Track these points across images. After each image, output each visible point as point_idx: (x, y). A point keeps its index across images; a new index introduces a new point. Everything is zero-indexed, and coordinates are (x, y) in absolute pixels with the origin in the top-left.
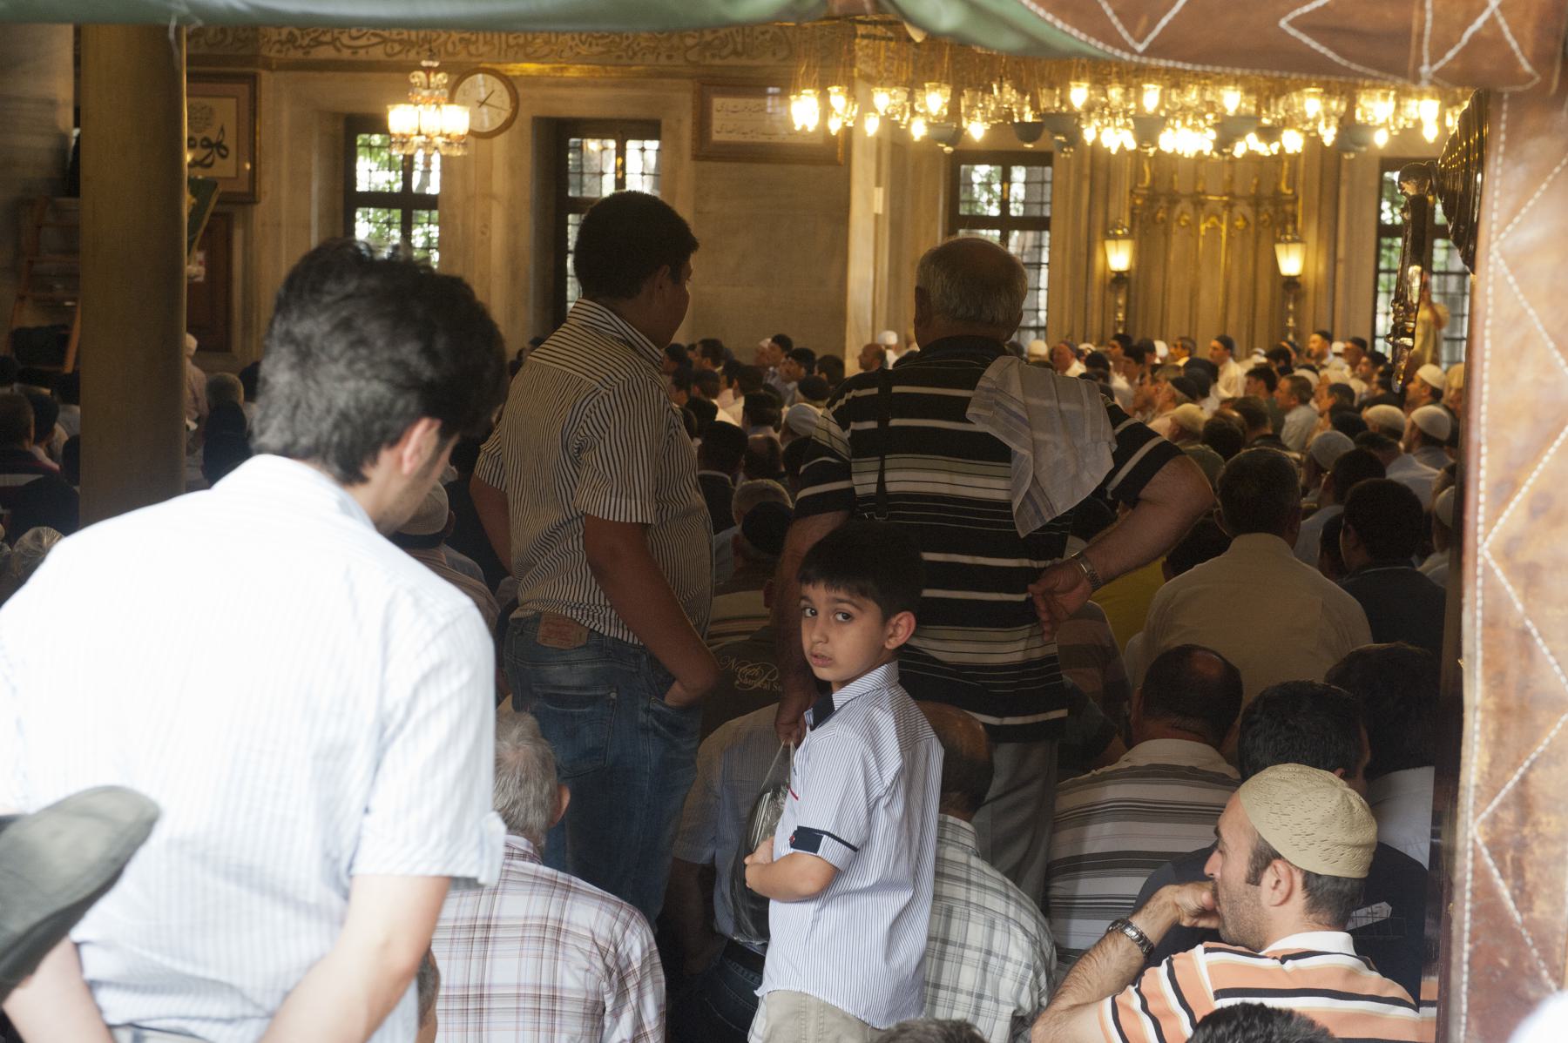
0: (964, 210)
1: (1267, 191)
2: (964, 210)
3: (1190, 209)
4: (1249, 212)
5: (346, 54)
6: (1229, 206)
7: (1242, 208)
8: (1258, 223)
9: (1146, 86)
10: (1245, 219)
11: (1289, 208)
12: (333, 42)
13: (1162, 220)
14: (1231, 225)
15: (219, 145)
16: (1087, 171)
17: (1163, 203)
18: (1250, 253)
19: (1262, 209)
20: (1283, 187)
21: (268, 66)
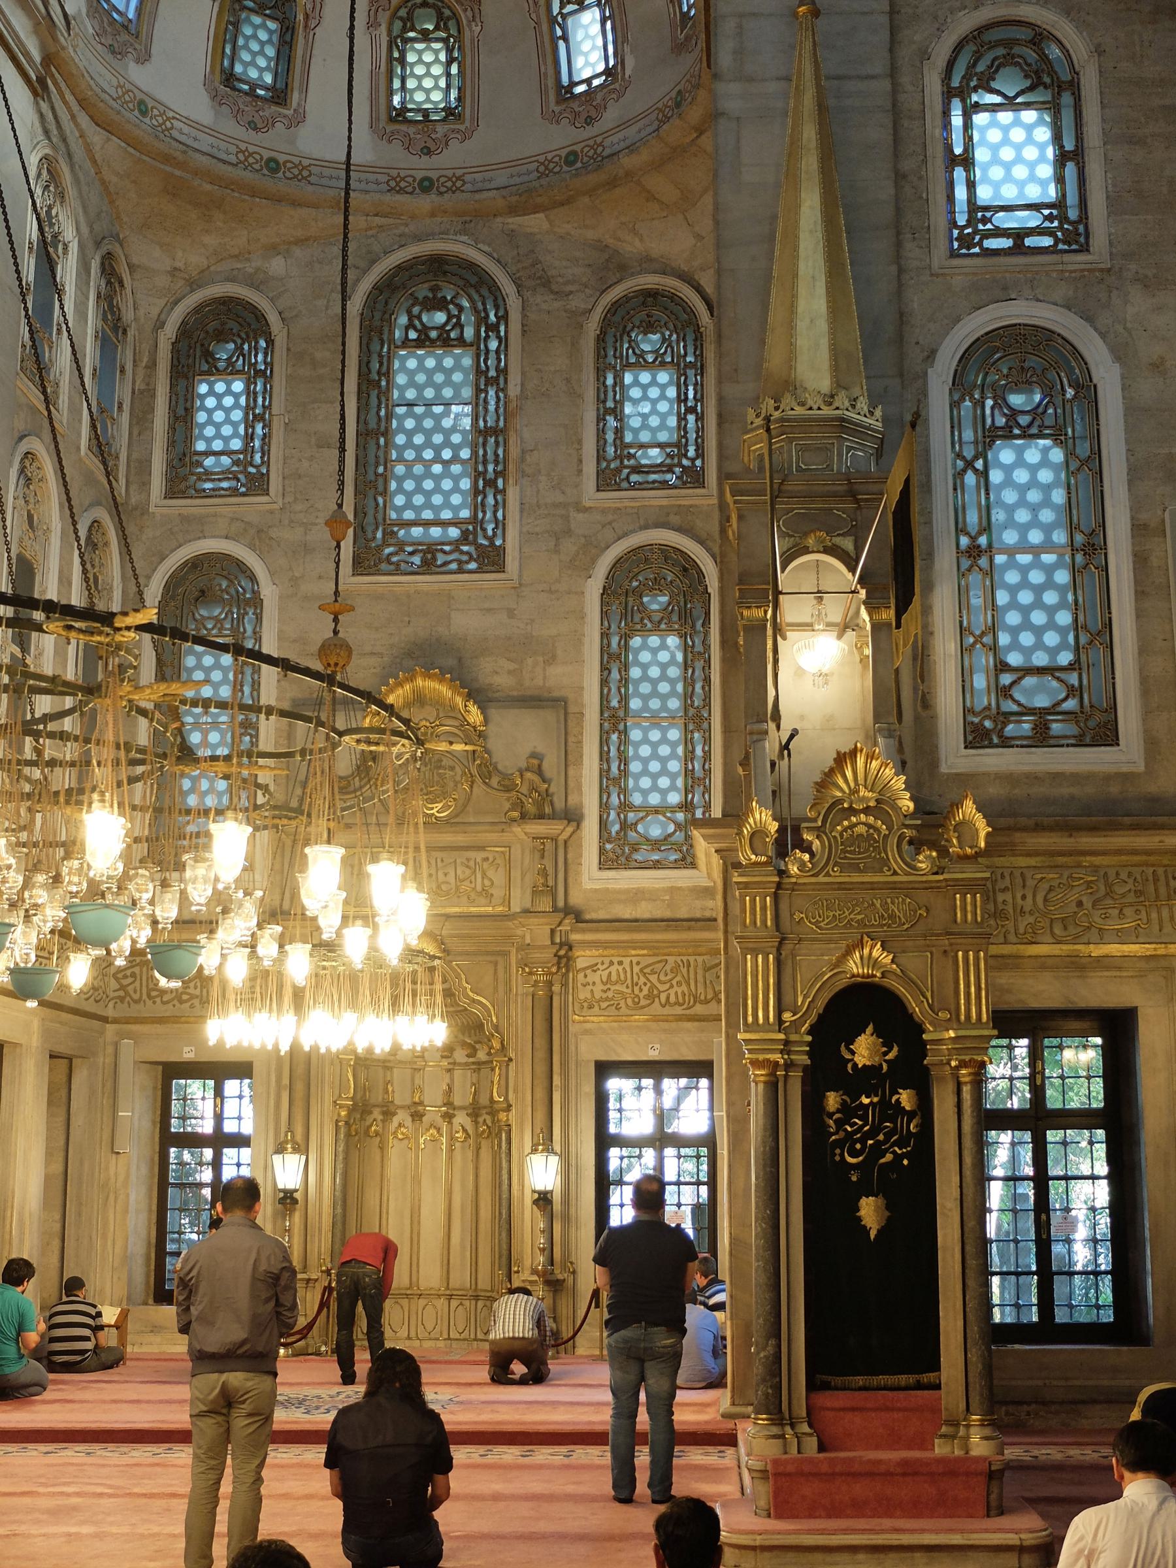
0: (175, 1126)
1: (484, 1100)
2: (175, 1126)
3: (408, 1121)
4: (468, 1123)
6: (448, 1117)
7: (461, 1119)
8: (479, 1135)
10: (465, 1130)
11: (502, 1116)
13: (377, 1134)
14: (452, 1138)
16: (286, 1081)
17: (377, 1114)
18: (471, 1166)
19: (481, 1120)
20: (496, 1098)
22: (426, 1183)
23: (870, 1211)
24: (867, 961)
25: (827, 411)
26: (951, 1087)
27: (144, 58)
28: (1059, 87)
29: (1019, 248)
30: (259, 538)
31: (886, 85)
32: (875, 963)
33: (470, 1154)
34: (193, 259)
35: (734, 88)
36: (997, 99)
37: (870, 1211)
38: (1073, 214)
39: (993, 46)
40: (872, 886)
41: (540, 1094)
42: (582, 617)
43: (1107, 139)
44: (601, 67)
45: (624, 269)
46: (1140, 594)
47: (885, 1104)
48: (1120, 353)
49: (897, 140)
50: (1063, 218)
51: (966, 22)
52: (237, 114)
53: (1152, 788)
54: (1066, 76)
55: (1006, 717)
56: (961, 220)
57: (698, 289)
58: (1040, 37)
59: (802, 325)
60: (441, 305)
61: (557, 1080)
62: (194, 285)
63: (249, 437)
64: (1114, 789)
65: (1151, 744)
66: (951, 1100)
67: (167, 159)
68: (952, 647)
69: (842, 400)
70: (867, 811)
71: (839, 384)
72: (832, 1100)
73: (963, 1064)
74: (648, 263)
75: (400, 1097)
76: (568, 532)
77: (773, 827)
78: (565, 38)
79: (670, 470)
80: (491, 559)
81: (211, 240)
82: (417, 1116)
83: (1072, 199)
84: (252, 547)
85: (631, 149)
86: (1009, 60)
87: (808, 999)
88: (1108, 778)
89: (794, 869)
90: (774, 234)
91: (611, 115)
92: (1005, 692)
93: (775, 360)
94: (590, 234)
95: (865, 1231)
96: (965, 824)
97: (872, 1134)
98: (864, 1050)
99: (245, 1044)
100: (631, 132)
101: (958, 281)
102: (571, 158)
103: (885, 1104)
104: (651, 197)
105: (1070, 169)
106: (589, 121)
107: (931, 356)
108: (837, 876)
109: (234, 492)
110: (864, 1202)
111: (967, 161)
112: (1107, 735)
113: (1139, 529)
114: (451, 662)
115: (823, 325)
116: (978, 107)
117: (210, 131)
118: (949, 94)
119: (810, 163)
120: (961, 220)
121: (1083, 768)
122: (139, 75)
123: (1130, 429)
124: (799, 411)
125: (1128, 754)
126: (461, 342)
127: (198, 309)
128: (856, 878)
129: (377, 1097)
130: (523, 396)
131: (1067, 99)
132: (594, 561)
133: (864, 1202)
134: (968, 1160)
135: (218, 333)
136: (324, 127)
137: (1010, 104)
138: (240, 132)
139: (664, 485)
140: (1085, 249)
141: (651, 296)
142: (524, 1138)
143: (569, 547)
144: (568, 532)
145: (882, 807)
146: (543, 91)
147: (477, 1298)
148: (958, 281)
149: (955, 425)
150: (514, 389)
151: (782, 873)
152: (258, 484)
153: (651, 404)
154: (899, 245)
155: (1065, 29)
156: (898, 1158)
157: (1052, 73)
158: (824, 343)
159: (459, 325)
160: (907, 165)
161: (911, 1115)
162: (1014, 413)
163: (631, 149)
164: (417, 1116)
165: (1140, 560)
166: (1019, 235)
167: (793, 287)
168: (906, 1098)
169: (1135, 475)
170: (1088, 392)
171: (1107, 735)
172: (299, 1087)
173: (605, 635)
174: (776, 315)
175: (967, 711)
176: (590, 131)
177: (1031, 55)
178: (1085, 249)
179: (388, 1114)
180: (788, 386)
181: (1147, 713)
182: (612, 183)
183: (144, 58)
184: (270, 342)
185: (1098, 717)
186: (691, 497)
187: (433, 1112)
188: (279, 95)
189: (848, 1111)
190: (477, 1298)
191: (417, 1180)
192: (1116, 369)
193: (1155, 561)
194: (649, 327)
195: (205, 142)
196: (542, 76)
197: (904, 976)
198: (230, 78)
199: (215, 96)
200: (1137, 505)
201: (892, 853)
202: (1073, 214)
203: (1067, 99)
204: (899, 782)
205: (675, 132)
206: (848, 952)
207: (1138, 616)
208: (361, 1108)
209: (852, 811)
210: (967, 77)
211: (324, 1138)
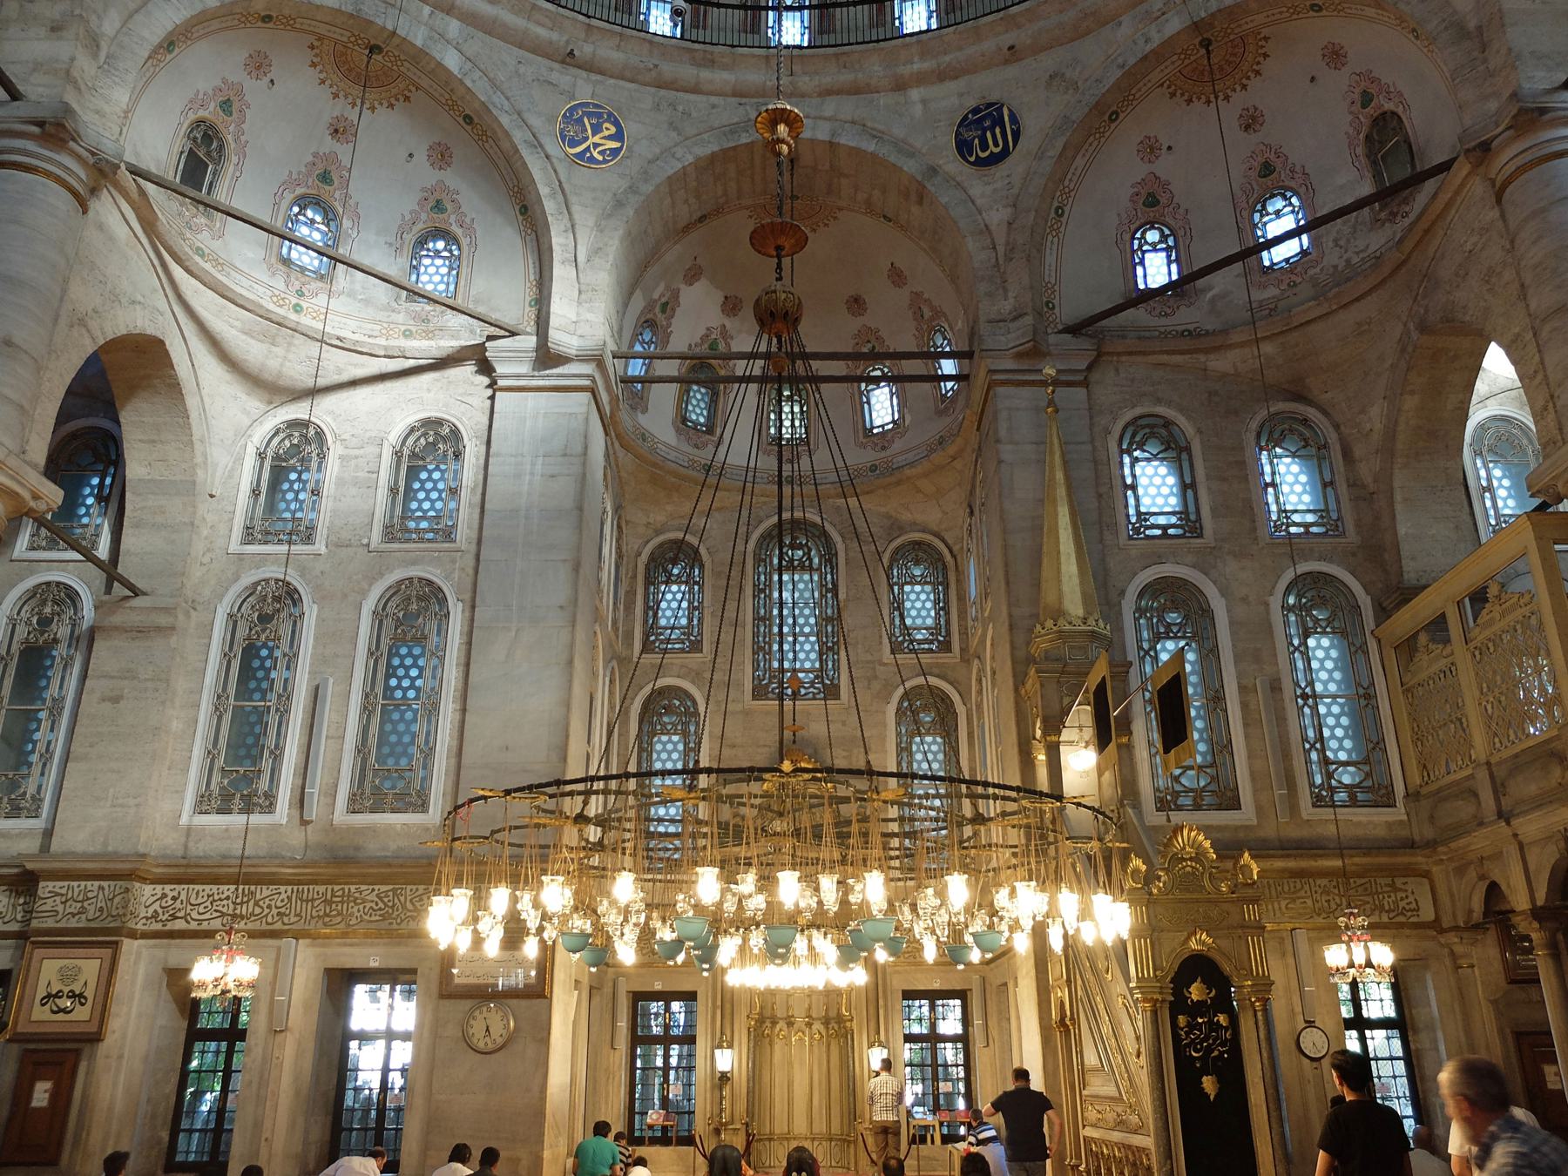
1: (833, 1014)
5: (193, 926)
6: (809, 1025)
7: (817, 1026)
9: (780, 875)
12: (184, 918)
14: (811, 1038)
15: (81, 996)
21: (133, 935)
22: (796, 1066)
23: (1209, 1084)
24: (1199, 942)
25: (1083, 628)
26: (1251, 1013)
27: (645, 410)
28: (1181, 450)
29: (1165, 535)
30: (696, 677)
31: (1089, 447)
32: (1203, 943)
33: (824, 1049)
34: (659, 518)
35: (1009, 447)
36: (1147, 455)
37: (1209, 1084)
38: (1193, 517)
39: (1143, 427)
40: (1197, 901)
41: (872, 1011)
42: (885, 725)
43: (1208, 477)
44: (889, 419)
45: (902, 530)
46: (1246, 725)
47: (1210, 1022)
48: (1224, 592)
49: (1097, 477)
50: (1188, 520)
51: (1129, 415)
52: (689, 439)
53: (1262, 834)
54: (1183, 444)
55: (1176, 794)
56: (1133, 520)
57: (943, 540)
58: (1168, 424)
59: (1065, 579)
60: (800, 547)
61: (881, 1002)
62: (658, 532)
63: (690, 620)
64: (1241, 835)
65: (1259, 810)
66: (1251, 1023)
67: (655, 465)
68: (1145, 754)
69: (1091, 621)
70: (1191, 859)
71: (1088, 613)
72: (1182, 1020)
73: (1258, 1000)
74: (914, 526)
75: (780, 1013)
76: (876, 677)
77: (1144, 868)
78: (868, 403)
79: (931, 642)
80: (831, 692)
81: (669, 508)
82: (790, 1024)
83: (1192, 508)
84: (693, 682)
85: (911, 464)
86: (1153, 435)
87: (1170, 965)
88: (1237, 828)
89: (1155, 891)
90: (1039, 530)
91: (898, 445)
92: (1176, 779)
93: (1049, 597)
94: (883, 510)
95: (1208, 1096)
96: (1247, 866)
97: (1206, 1039)
98: (1196, 992)
99: (773, 987)
100: (910, 456)
101: (1134, 552)
102: (873, 468)
103: (1210, 1022)
104: (919, 491)
105: (1190, 493)
106: (884, 448)
107: (1122, 593)
108: (1178, 895)
109: (682, 651)
110: (1205, 1079)
111: (1134, 487)
112: (1235, 805)
113: (1243, 689)
114: (810, 751)
115: (1076, 580)
116: (1137, 460)
117: (676, 449)
118: (1122, 452)
119: (1061, 492)
120: (1133, 520)
121: (1223, 823)
122: (642, 419)
123: (1233, 634)
124: (1068, 627)
125: (1247, 815)
126: (811, 569)
127: (661, 545)
128: (1188, 896)
129: (768, 1013)
130: (847, 600)
131: (1184, 456)
132: (890, 695)
133: (1205, 1079)
134: (1265, 1055)
135: (674, 557)
136: (739, 448)
137: (1155, 457)
138: (690, 450)
139: (931, 651)
140: (1200, 536)
141: (918, 544)
142: (861, 1039)
143: (876, 686)
144: (876, 677)
145: (1199, 856)
146: (856, 432)
147: (831, 1140)
148: (1134, 552)
149: (1138, 630)
150: (842, 596)
151: (1151, 894)
152: (696, 646)
153: (920, 605)
154: (1101, 532)
155: (1182, 421)
156: (1222, 1053)
157: (1176, 442)
158: (1078, 589)
159: (810, 559)
160: (1103, 490)
161: (1226, 1029)
162: (1169, 626)
163: (911, 464)
164: (790, 1024)
165: (1244, 706)
166: (1165, 528)
167: (1058, 559)
168: (1222, 1019)
169: (1238, 659)
170: (1207, 613)
171: (1235, 805)
172: (728, 1006)
173: (899, 734)
174: (1047, 572)
175: (1157, 790)
176: (883, 454)
177: (1163, 432)
178: (1200, 536)
179: (774, 1023)
180: (1058, 613)
181: (1255, 791)
182: (898, 483)
183: (645, 410)
184: (702, 567)
185: (1229, 794)
186: (944, 658)
187: (800, 1021)
188: (710, 430)
189: (1192, 1026)
190: (831, 1140)
191: (790, 1064)
192: (1223, 601)
193: (1252, 707)
194: (917, 563)
195: (672, 455)
196: (855, 423)
197: (1219, 950)
198: (684, 420)
199: (678, 430)
200: (1240, 676)
201: (1206, 883)
202: (1193, 517)
203: (1184, 456)
204: (1207, 844)
205: (938, 458)
206: (1188, 938)
207: (1246, 737)
208: (761, 1021)
209: (1184, 860)
210: (1131, 444)
211: (742, 1037)
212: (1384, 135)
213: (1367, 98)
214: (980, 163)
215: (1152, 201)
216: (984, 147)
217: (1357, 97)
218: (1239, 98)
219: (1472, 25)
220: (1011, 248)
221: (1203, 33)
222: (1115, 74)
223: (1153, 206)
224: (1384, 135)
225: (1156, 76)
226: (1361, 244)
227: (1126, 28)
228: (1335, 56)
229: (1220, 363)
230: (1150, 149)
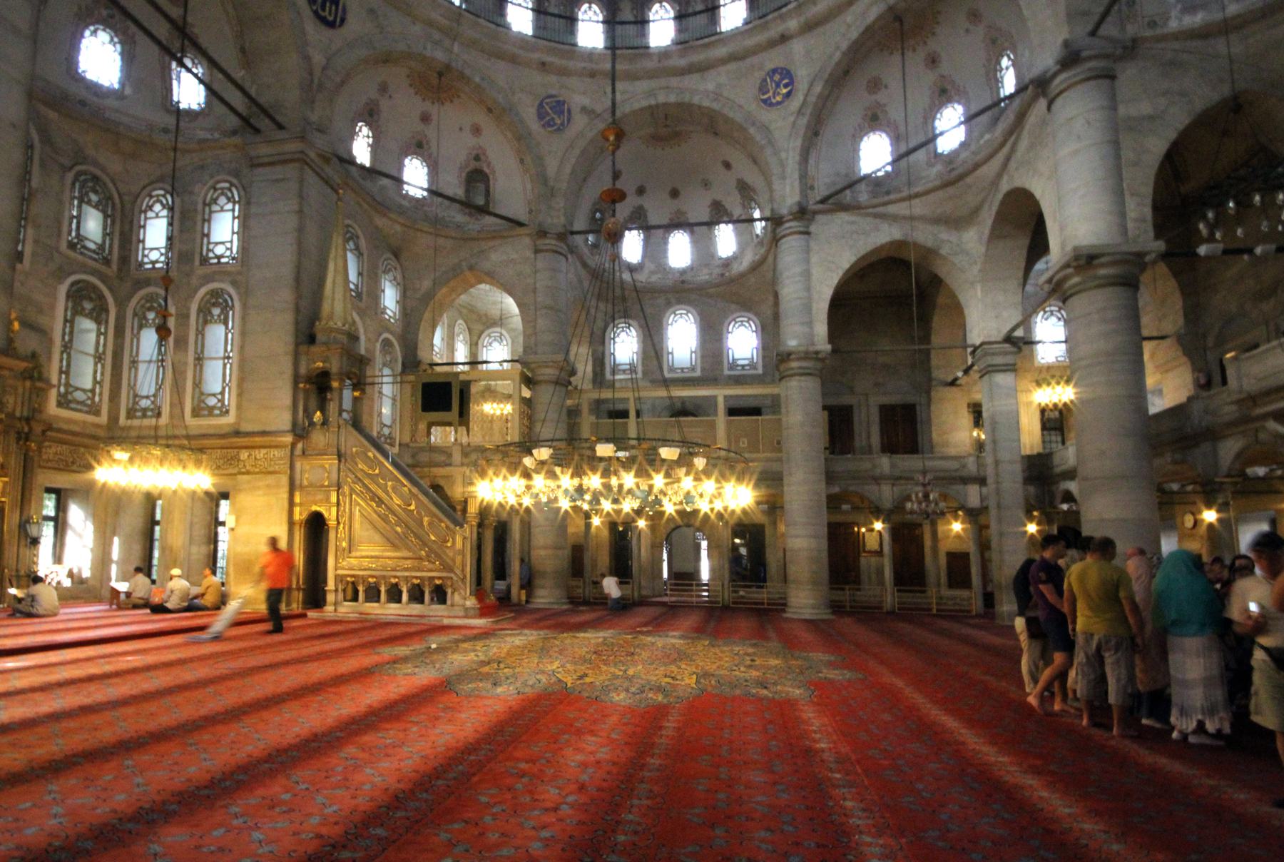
212: (477, 177)
213: (477, 158)
214: (316, 13)
215: (371, 115)
216: (324, 10)
217: (475, 152)
218: (428, 103)
219: (551, 183)
220: (321, 86)
221: (444, 72)
222: (401, 46)
223: (371, 116)
224: (477, 177)
225: (413, 64)
226: (452, 214)
227: (417, 29)
228: (477, 130)
229: (380, 222)
230: (383, 88)
